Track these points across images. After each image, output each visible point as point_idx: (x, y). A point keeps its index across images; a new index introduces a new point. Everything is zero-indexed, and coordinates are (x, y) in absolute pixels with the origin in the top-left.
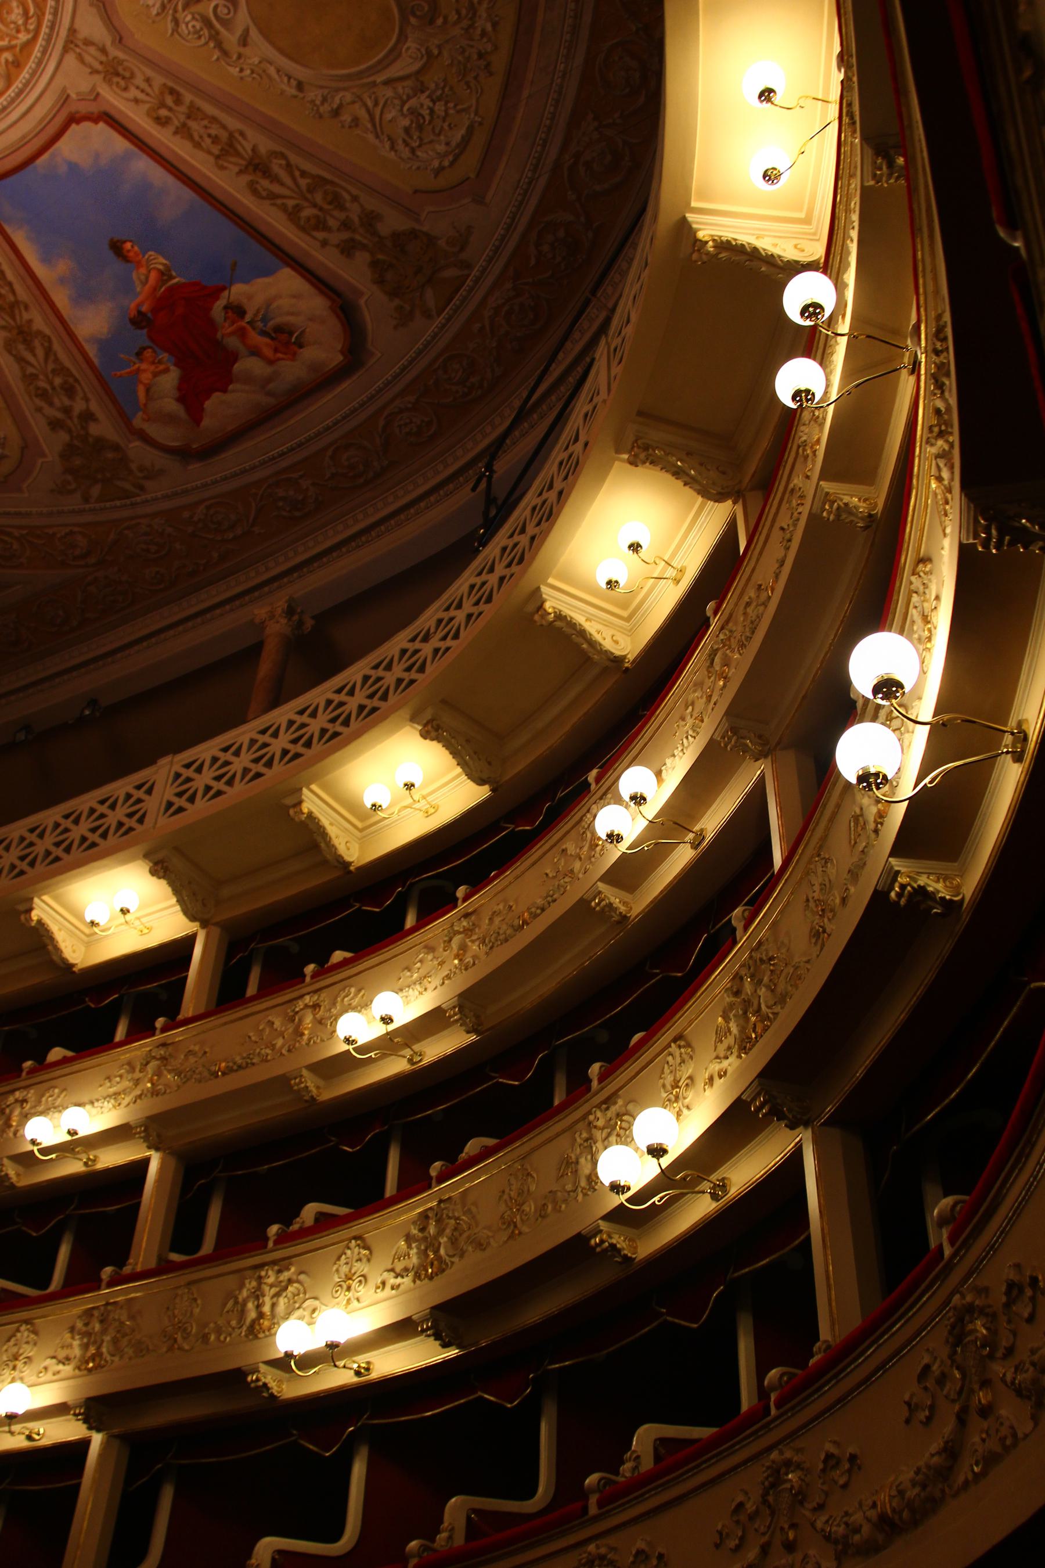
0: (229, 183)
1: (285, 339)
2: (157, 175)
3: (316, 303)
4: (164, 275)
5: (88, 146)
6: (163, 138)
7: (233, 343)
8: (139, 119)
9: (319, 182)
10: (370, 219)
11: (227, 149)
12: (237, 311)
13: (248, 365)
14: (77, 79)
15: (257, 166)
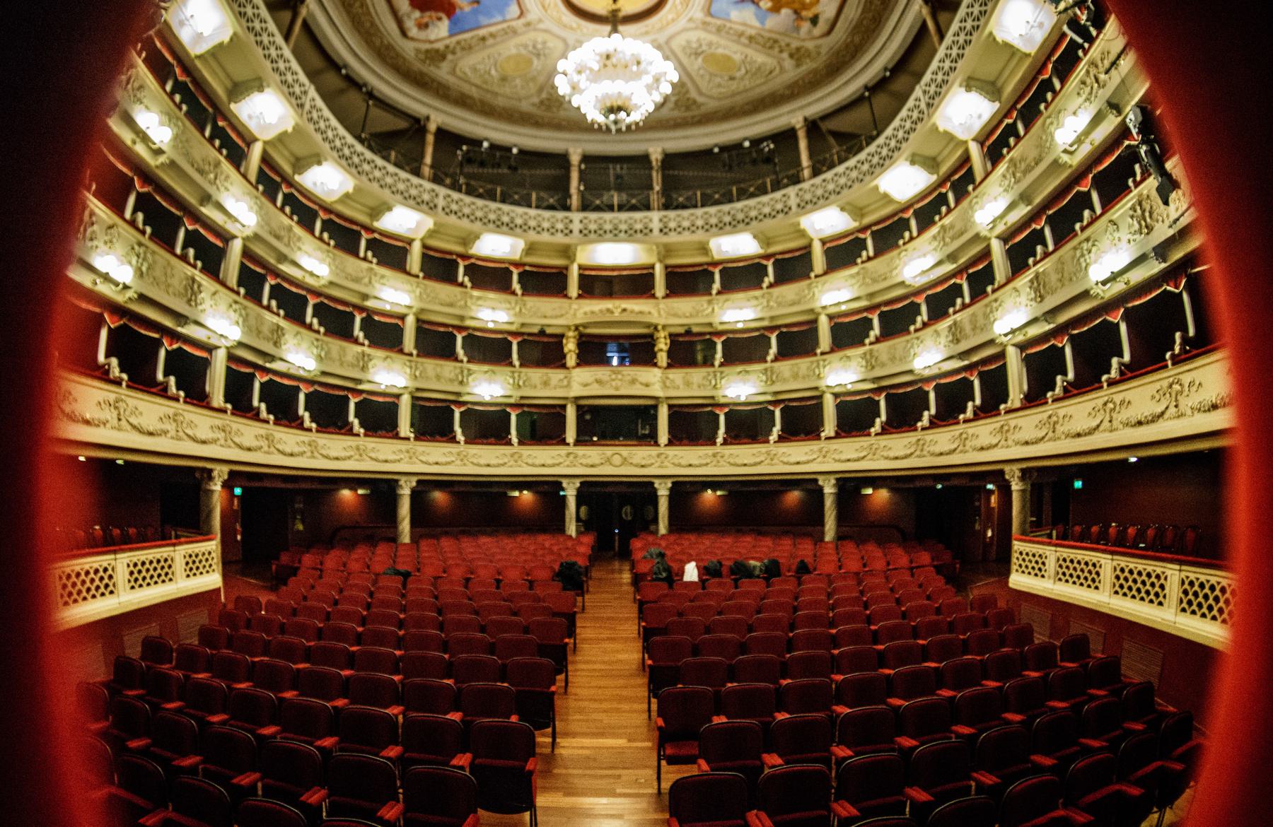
0: (482, 32)
1: (423, 26)
2: (494, 20)
3: (433, 37)
4: (461, 9)
5: (514, 10)
6: (505, 25)
7: (428, 14)
8: (514, 24)
9: (470, 48)
10: (454, 53)
11: (492, 35)
12: (440, 19)
13: (417, 14)
14: (531, 17)
15: (483, 39)
